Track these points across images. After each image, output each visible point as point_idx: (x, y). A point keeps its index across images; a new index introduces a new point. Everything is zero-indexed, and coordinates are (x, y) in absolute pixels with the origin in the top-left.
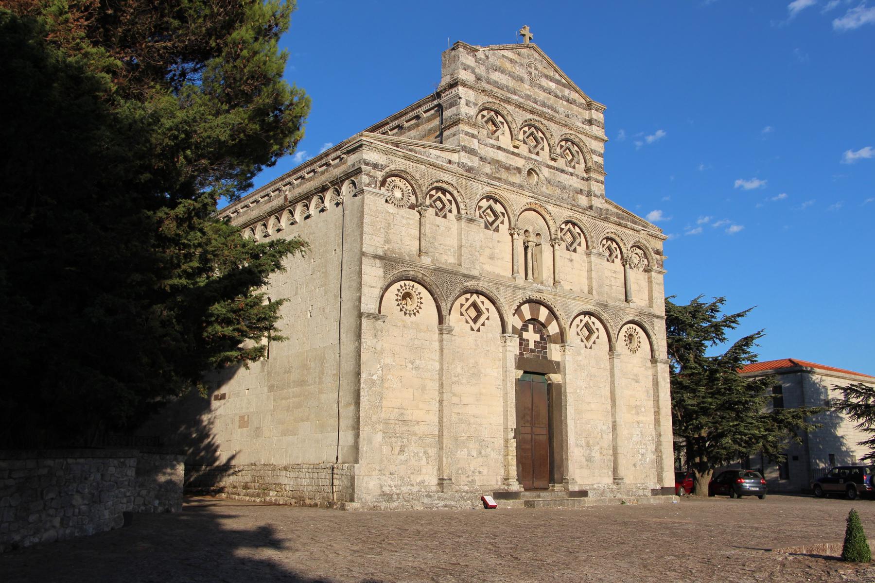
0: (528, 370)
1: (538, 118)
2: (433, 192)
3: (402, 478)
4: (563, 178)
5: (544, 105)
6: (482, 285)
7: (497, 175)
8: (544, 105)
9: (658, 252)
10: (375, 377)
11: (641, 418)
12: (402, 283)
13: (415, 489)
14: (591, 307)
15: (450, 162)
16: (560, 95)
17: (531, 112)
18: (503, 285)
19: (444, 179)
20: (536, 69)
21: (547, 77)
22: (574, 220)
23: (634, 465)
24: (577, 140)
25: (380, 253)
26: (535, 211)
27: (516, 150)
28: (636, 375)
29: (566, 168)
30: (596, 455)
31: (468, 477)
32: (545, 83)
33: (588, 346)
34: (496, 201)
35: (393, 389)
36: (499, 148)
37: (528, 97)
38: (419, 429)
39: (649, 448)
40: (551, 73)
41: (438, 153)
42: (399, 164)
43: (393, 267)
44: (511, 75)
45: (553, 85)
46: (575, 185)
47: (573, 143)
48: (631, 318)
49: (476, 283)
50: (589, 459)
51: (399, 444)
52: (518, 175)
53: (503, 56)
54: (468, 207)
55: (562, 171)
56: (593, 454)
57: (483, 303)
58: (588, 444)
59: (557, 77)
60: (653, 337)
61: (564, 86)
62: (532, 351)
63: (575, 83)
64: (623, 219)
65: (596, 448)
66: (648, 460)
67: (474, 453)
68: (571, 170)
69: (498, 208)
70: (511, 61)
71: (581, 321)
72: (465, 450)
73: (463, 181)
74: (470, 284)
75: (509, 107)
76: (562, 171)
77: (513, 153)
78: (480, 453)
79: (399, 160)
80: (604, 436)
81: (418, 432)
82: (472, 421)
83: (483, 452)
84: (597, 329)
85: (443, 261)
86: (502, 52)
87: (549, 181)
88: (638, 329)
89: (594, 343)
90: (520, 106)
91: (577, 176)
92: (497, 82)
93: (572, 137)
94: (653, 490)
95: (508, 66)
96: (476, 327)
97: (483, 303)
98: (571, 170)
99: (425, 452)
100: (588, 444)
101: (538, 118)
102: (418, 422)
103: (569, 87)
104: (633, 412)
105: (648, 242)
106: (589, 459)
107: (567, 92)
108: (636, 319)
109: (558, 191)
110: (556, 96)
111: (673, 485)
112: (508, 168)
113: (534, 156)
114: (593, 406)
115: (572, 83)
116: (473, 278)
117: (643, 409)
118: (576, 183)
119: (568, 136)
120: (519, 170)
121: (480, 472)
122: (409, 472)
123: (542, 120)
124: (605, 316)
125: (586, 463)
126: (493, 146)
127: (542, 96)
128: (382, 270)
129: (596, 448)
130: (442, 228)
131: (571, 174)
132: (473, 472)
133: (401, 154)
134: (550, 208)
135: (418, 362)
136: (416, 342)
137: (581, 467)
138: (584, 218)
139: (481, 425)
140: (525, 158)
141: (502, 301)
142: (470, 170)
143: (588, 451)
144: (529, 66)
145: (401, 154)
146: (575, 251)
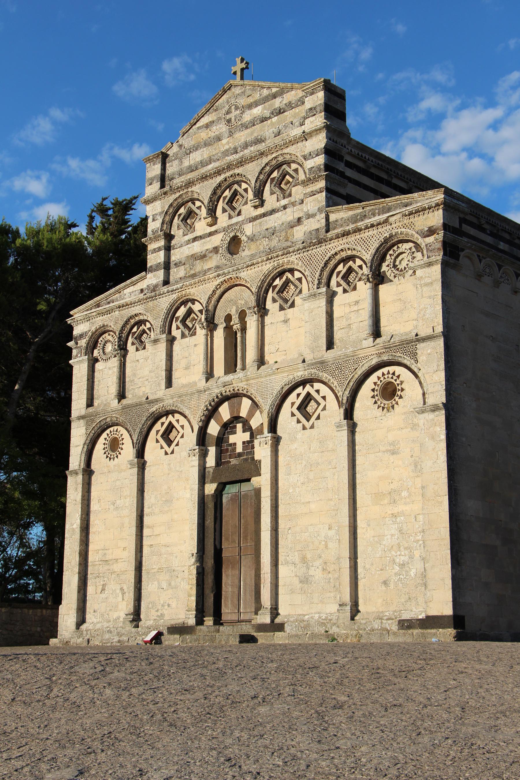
0: (224, 480)
1: (228, 174)
2: (135, 329)
3: (102, 615)
4: (272, 221)
5: (246, 146)
6: (168, 403)
7: (192, 272)
8: (246, 146)
9: (431, 232)
10: (75, 526)
11: (400, 508)
12: (108, 431)
13: (111, 624)
15: (142, 291)
16: (267, 114)
18: (186, 395)
19: (134, 313)
20: (237, 108)
21: (250, 106)
23: (385, 583)
24: (288, 157)
25: (83, 412)
26: (237, 285)
27: (213, 229)
28: (392, 444)
30: (316, 573)
31: (157, 611)
32: (247, 117)
33: (169, 452)
34: (193, 301)
35: (99, 533)
36: (195, 239)
37: (226, 153)
38: (116, 567)
39: (417, 554)
40: (257, 96)
41: (131, 289)
42: (99, 321)
43: (93, 421)
44: (207, 144)
45: (257, 111)
46: (290, 218)
47: (288, 163)
48: (375, 361)
50: (305, 580)
51: (102, 583)
52: (215, 256)
53: (199, 128)
55: (273, 212)
56: (311, 572)
57: (178, 421)
58: (304, 560)
59: (265, 92)
60: (420, 375)
61: (274, 96)
62: (240, 455)
63: (284, 82)
64: (364, 217)
65: (317, 563)
66: (412, 573)
67: (164, 585)
68: (284, 202)
69: (197, 307)
70: (207, 126)
71: (298, 395)
72: (156, 583)
73: (151, 304)
75: (196, 188)
76: (273, 212)
77: (211, 234)
78: (170, 584)
79: (97, 319)
80: (330, 545)
81: (116, 570)
82: (163, 550)
83: (173, 583)
84: (324, 398)
85: (141, 394)
86: (198, 125)
87: (252, 239)
89: (299, 422)
90: (204, 178)
91: (293, 204)
92: (190, 167)
93: (281, 159)
94: (400, 621)
95: (204, 135)
96: (169, 451)
97: (178, 421)
99: (122, 589)
100: (304, 560)
101: (228, 174)
102: (117, 560)
103: (281, 93)
104: (386, 501)
105: (411, 225)
106: (305, 580)
107: (277, 103)
108: (385, 358)
109: (265, 242)
110: (264, 120)
111: (448, 610)
112: (203, 257)
113: (235, 220)
114: (313, 506)
115: (282, 85)
116: (157, 401)
117: (404, 494)
118: (290, 215)
119: (274, 162)
120: (216, 250)
121: (169, 605)
122: (108, 609)
123: (237, 171)
124: (324, 376)
125: (299, 586)
126: (188, 242)
127: (242, 136)
128: (84, 428)
129: (317, 563)
130: (141, 361)
131: (285, 207)
132: (163, 606)
133: (94, 314)
134: (243, 274)
135: (118, 502)
136: (118, 483)
137: (292, 592)
138: (293, 258)
139: (171, 554)
140: (224, 230)
141: (187, 413)
142: (154, 288)
143: (304, 570)
144: (228, 112)
145: (94, 314)
146: (292, 305)
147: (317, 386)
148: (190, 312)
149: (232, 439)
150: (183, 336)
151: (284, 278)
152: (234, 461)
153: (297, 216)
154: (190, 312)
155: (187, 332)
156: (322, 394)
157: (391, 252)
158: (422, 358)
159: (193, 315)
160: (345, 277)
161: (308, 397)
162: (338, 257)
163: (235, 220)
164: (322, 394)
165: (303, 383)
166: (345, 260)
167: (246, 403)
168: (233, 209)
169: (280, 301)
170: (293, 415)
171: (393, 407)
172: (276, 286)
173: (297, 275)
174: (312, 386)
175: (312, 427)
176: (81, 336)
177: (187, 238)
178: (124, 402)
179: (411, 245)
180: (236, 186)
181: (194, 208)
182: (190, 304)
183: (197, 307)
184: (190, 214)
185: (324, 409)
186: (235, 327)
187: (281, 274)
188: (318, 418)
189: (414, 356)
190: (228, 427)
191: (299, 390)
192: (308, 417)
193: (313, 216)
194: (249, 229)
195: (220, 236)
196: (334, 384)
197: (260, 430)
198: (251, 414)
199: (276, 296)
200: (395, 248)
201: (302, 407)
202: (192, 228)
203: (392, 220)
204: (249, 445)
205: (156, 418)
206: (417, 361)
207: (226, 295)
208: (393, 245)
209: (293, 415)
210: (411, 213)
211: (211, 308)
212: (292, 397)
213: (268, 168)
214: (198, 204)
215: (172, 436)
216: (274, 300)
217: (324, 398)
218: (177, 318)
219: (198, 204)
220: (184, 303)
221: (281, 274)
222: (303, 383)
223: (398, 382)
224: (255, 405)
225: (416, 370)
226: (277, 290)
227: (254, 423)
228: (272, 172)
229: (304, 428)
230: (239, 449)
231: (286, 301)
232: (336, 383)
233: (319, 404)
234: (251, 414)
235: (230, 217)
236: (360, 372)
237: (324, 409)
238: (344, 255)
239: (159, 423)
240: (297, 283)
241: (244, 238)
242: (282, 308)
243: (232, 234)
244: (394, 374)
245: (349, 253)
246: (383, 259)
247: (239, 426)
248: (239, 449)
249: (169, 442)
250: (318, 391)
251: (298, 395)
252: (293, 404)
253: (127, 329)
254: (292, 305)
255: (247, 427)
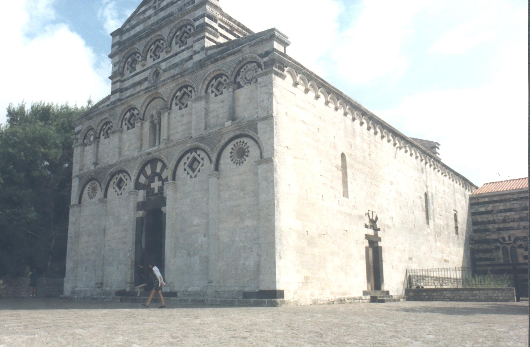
2: (104, 127)
4: (177, 59)
14: (189, 145)
17: (148, 35)
22: (183, 84)
24: (185, 22)
29: (179, 50)
48: (232, 135)
49: (115, 167)
54: (115, 124)
55: (176, 54)
62: (157, 194)
68: (183, 48)
69: (136, 112)
74: (112, 170)
75: (137, 46)
84: (202, 159)
87: (165, 71)
88: (246, 140)
91: (188, 48)
93: (181, 24)
98: (183, 48)
101: (153, 36)
108: (238, 132)
113: (156, 61)
118: (186, 54)
120: (146, 79)
124: (202, 145)
127: (162, 14)
140: (151, 67)
147: (199, 152)
148: (133, 115)
149: (152, 185)
150: (128, 129)
151: (182, 91)
152: (152, 198)
153: (189, 55)
154: (133, 115)
155: (130, 127)
156: (201, 157)
157: (243, 70)
158: (259, 131)
159: (134, 117)
160: (217, 88)
161: (195, 159)
162: (212, 76)
163: (156, 61)
164: (201, 157)
165: (191, 150)
166: (216, 77)
167: (159, 165)
168: (156, 55)
169: (180, 104)
170: (185, 170)
171: (243, 162)
172: (177, 96)
173: (189, 89)
174: (196, 152)
175: (196, 176)
176: (79, 132)
177: (132, 74)
178: (97, 167)
179: (255, 64)
180: (158, 43)
181: (136, 58)
182: (132, 111)
183: (136, 112)
184: (135, 61)
185: (202, 165)
186: (155, 121)
187: (180, 89)
188: (199, 171)
189: (256, 131)
190: (151, 179)
191: (189, 155)
192: (193, 170)
193: (198, 52)
194: (164, 66)
195: (149, 71)
196: (208, 149)
197: (166, 179)
198: (162, 170)
199: (178, 102)
200: (245, 67)
201: (191, 166)
202: (134, 69)
203: (243, 49)
204: (161, 189)
205: (112, 176)
206: (257, 133)
207: (151, 104)
208: (244, 65)
209: (185, 170)
210: (255, 44)
211: (142, 112)
212: (184, 160)
213: (174, 30)
214: (138, 55)
215: (121, 185)
216: (177, 104)
217: (202, 159)
218: (126, 119)
219: (138, 55)
220: (129, 110)
221: (180, 89)
222: (191, 150)
223: (246, 147)
224: (164, 166)
225: (256, 139)
226: (178, 98)
227: (164, 176)
228: (176, 32)
229: (191, 177)
230: (156, 191)
231: (183, 104)
232: (209, 149)
233: (199, 163)
234: (162, 170)
235: (154, 60)
236: (223, 142)
237: (202, 165)
238: (215, 74)
239: (115, 177)
240: (189, 93)
241: (161, 71)
242: (180, 109)
243: (154, 70)
244: (243, 142)
245: (219, 72)
246: (238, 74)
247: (156, 178)
248: (156, 191)
249: (120, 188)
250: (199, 155)
251: (188, 158)
252: (185, 163)
253: (100, 127)
254: (186, 106)
255: (160, 179)
